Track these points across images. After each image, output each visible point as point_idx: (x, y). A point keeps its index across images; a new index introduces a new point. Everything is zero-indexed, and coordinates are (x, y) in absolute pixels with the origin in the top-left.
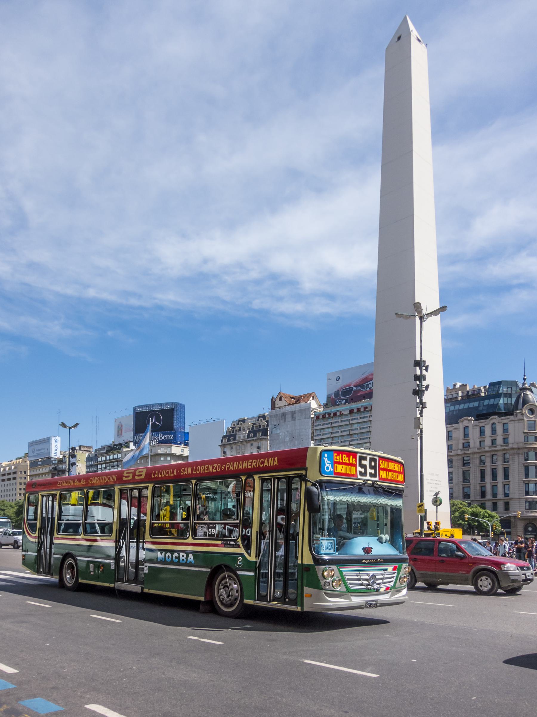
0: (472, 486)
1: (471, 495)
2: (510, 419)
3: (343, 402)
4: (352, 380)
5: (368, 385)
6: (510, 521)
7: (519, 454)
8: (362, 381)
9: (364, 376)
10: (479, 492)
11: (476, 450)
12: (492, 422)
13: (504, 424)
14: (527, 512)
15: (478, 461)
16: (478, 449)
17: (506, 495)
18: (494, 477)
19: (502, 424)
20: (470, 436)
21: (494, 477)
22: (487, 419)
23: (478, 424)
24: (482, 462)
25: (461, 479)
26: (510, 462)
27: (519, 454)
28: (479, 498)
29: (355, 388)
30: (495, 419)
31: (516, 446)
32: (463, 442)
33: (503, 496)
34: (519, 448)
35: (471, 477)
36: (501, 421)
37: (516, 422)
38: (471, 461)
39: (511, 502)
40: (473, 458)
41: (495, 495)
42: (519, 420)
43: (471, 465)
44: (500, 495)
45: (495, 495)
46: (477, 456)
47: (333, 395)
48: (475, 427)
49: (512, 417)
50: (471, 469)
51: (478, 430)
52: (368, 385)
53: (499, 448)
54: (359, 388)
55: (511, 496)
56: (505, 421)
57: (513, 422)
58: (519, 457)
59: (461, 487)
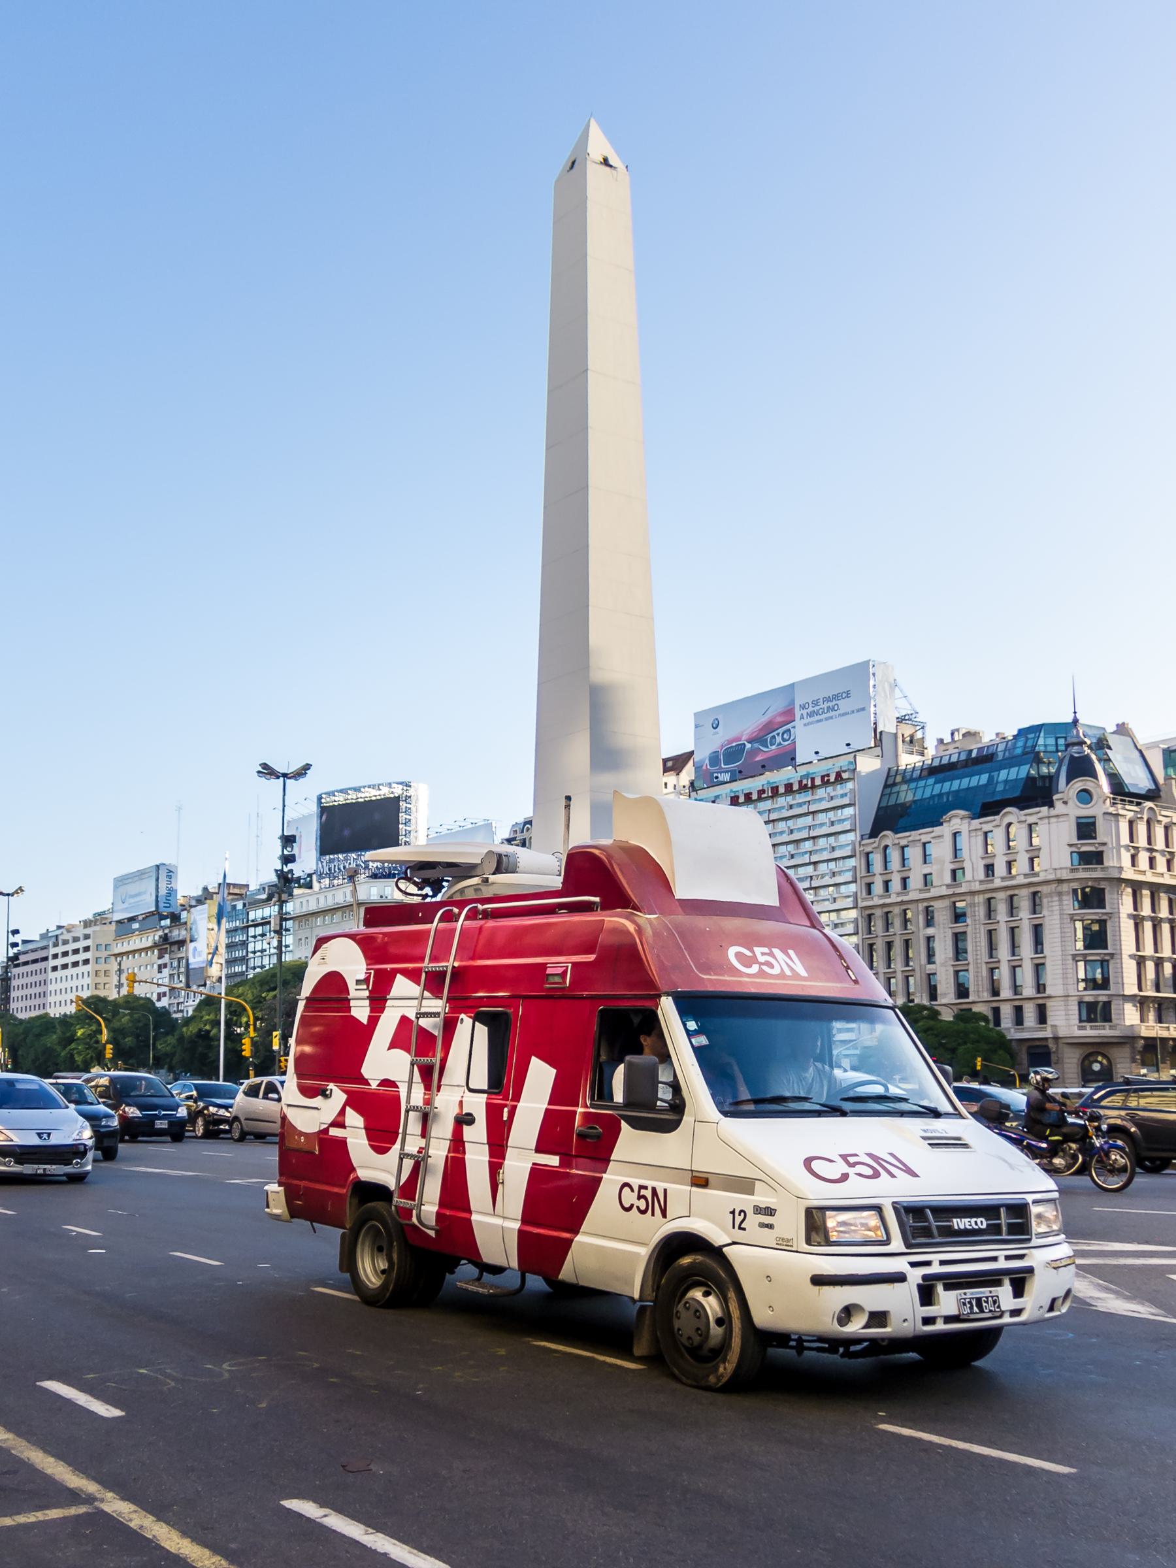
0: (971, 968)
1: (971, 990)
2: (1040, 815)
3: (726, 777)
4: (743, 728)
5: (774, 737)
6: (1047, 1046)
7: (1060, 894)
8: (761, 730)
9: (765, 719)
10: (986, 984)
11: (977, 887)
12: (1006, 820)
13: (1030, 826)
14: (1080, 1028)
15: (981, 911)
16: (981, 882)
17: (1040, 987)
18: (1014, 947)
19: (1025, 826)
20: (965, 854)
21: (1014, 947)
22: (997, 813)
23: (979, 826)
24: (990, 912)
25: (950, 953)
26: (1045, 912)
27: (1060, 894)
28: (986, 996)
29: (748, 746)
30: (1012, 814)
31: (1052, 877)
32: (953, 866)
33: (1034, 991)
34: (1060, 881)
35: (970, 948)
36: (1023, 818)
37: (1053, 820)
38: (969, 914)
39: (1050, 1004)
40: (973, 905)
41: (1016, 989)
42: (1057, 816)
43: (969, 921)
44: (1029, 990)
45: (1016, 989)
46: (980, 899)
47: (707, 762)
48: (973, 834)
49: (1045, 809)
50: (969, 930)
51: (980, 839)
52: (774, 737)
53: (1021, 880)
54: (756, 745)
55: (1049, 991)
56: (1031, 820)
57: (1046, 821)
58: (1060, 900)
59: (951, 970)
